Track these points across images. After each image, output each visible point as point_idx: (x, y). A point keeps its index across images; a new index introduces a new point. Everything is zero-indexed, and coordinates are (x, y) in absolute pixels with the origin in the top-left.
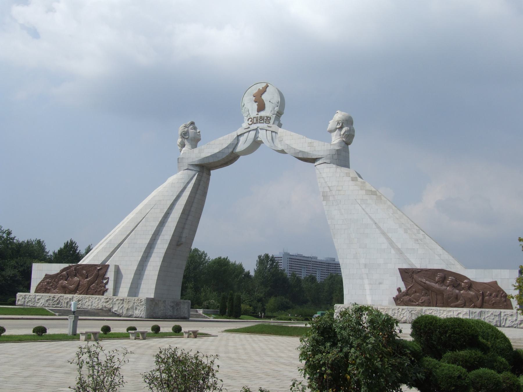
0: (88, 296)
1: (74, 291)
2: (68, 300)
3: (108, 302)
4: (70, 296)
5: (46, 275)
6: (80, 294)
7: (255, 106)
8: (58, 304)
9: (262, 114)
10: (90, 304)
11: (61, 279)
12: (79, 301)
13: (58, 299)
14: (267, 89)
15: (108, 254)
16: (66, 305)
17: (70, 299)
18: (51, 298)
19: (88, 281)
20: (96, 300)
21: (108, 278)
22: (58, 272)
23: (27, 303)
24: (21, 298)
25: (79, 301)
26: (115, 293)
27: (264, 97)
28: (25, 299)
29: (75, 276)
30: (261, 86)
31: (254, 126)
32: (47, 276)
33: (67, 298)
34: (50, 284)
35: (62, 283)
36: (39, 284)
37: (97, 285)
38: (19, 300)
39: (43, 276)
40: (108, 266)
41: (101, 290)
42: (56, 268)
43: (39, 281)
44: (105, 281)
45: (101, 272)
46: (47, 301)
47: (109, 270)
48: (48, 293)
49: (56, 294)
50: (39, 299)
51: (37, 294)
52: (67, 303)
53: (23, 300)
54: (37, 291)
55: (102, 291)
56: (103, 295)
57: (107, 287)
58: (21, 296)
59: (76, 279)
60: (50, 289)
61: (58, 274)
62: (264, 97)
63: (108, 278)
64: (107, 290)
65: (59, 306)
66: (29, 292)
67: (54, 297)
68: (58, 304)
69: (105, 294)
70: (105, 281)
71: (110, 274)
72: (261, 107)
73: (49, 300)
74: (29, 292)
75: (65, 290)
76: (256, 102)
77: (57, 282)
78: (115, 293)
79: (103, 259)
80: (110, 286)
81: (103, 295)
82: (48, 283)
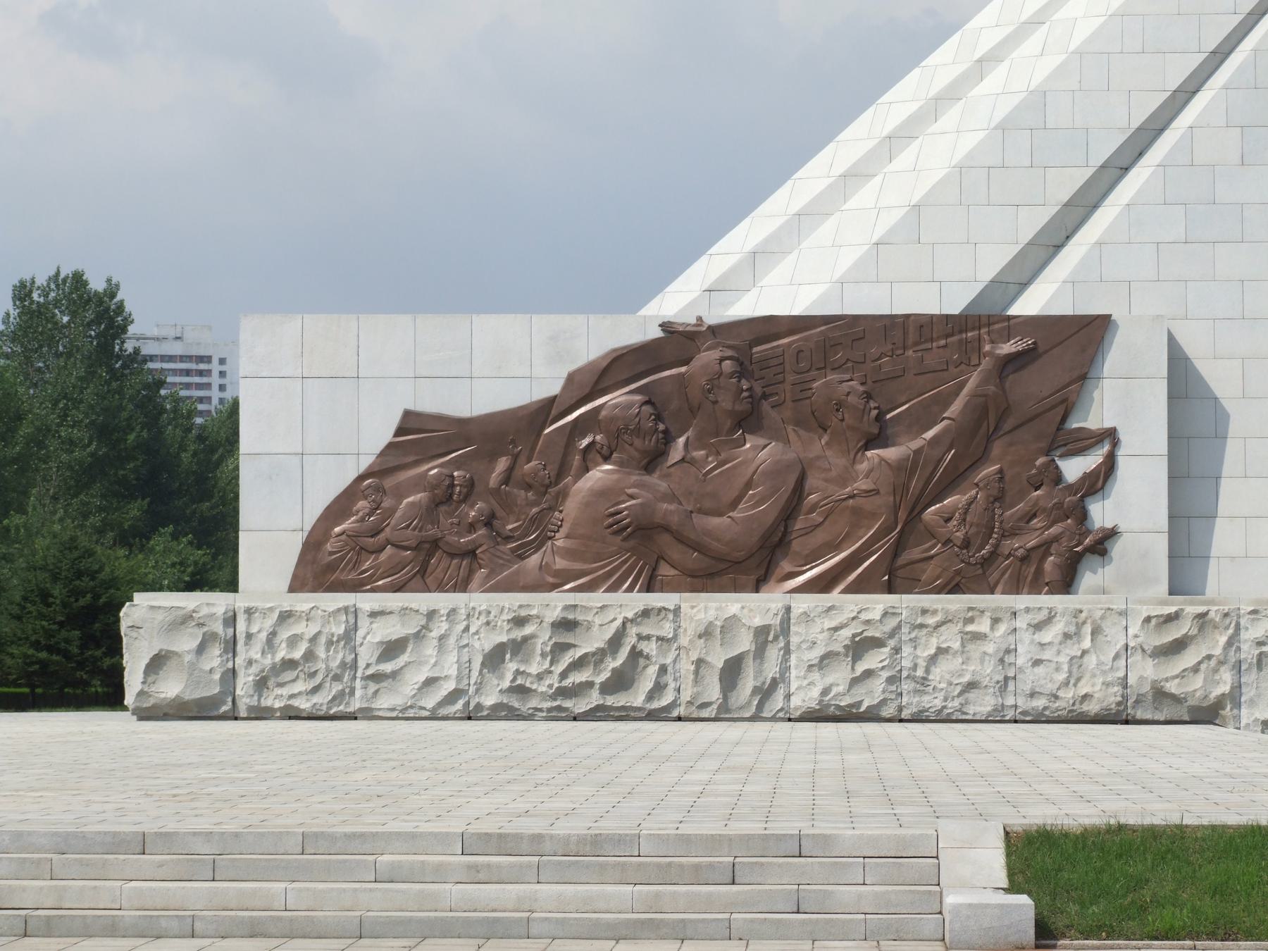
0: (906, 603)
1: (753, 565)
2: (744, 643)
3: (1178, 646)
4: (751, 608)
5: (411, 423)
6: (823, 584)
8: (620, 681)
10: (989, 672)
11: (589, 458)
12: (860, 647)
13: (615, 643)
15: (1032, 222)
16: (713, 692)
17: (762, 635)
18: (544, 640)
19: (906, 468)
20: (1051, 634)
21: (1110, 435)
22: (551, 386)
23: (261, 684)
24: (186, 643)
25: (860, 647)
26: (1185, 565)
28: (231, 646)
29: (748, 421)
32: (418, 434)
33: (730, 625)
34: (450, 505)
35: (602, 494)
36: (339, 508)
37: (999, 498)
38: (157, 663)
39: (378, 433)
41: (1045, 548)
42: (509, 362)
44: (1074, 468)
45: (1032, 386)
46: (494, 659)
47: (1115, 359)
48: (462, 586)
49: (597, 598)
50: (392, 649)
51: (304, 602)
52: (732, 671)
53: (214, 660)
54: (320, 568)
55: (1065, 551)
56: (1066, 584)
57: (1101, 513)
58: (185, 620)
59: (758, 452)
60: (471, 553)
61: (546, 410)
63: (1110, 435)
64: (1102, 544)
65: (637, 698)
67: (566, 625)
68: (620, 681)
69: (1089, 579)
70: (1074, 468)
71: (1125, 400)
73: (518, 647)
74: (232, 585)
75: (651, 551)
77: (549, 490)
78: (1185, 565)
79: (988, 273)
80: (1134, 503)
81: (1066, 584)
82: (444, 497)
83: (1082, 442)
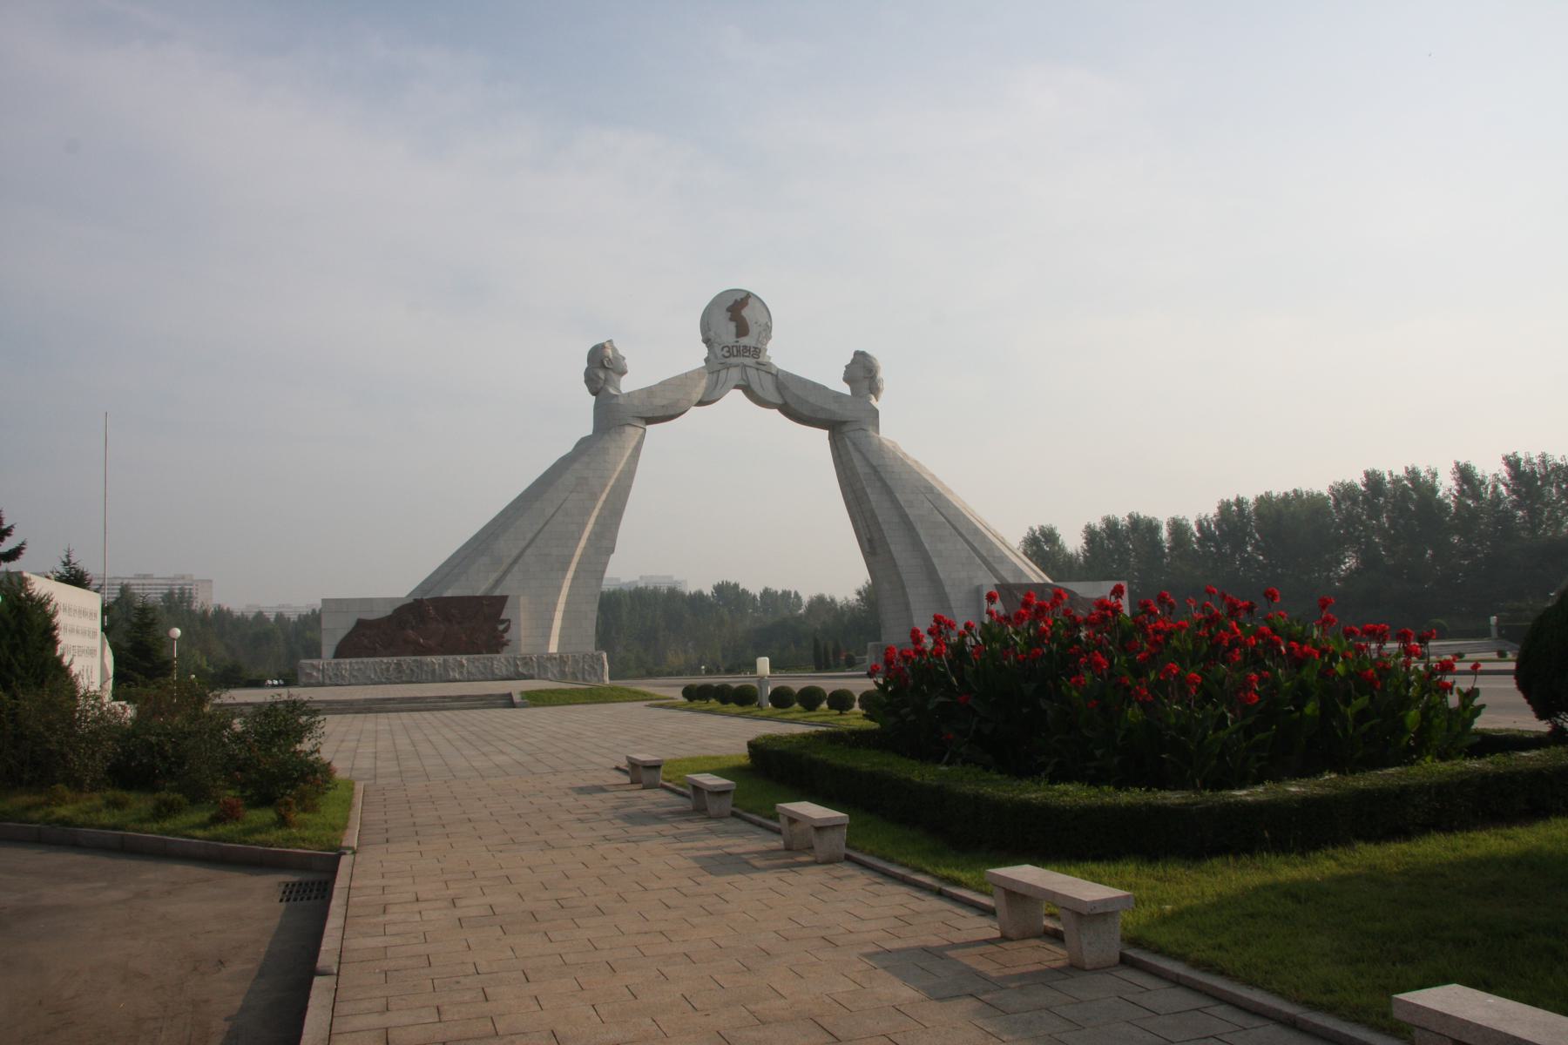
7: (732, 326)
9: (745, 341)
14: (751, 301)
27: (746, 313)
30: (739, 297)
31: (733, 360)
39: (351, 623)
40: (503, 600)
43: (342, 633)
44: (501, 627)
57: (507, 636)
61: (389, 619)
62: (746, 313)
64: (506, 644)
66: (319, 656)
69: (506, 648)
70: (501, 627)
72: (742, 330)
74: (319, 656)
76: (731, 319)
83: (503, 622)
